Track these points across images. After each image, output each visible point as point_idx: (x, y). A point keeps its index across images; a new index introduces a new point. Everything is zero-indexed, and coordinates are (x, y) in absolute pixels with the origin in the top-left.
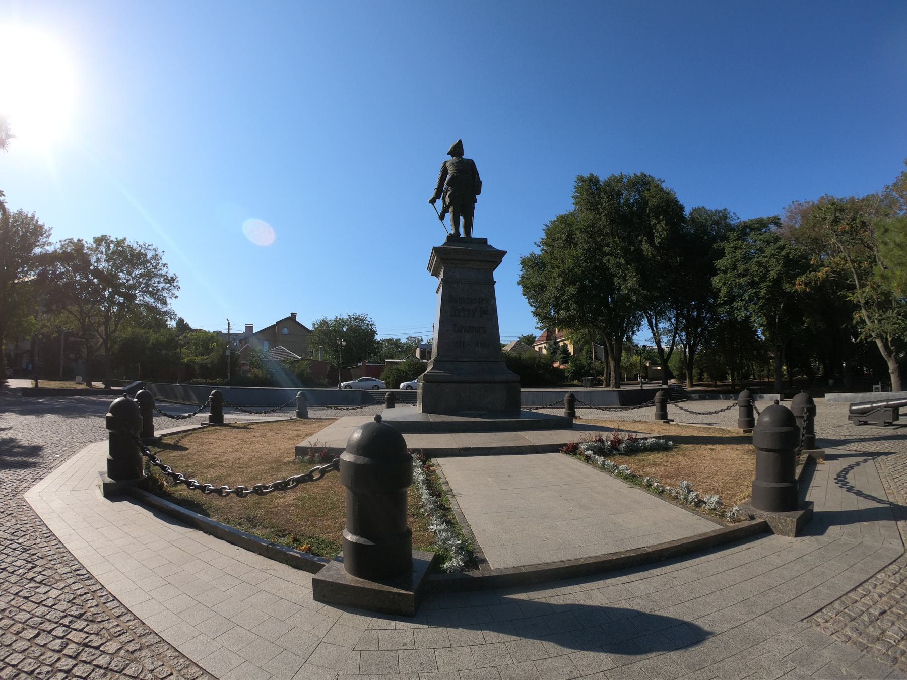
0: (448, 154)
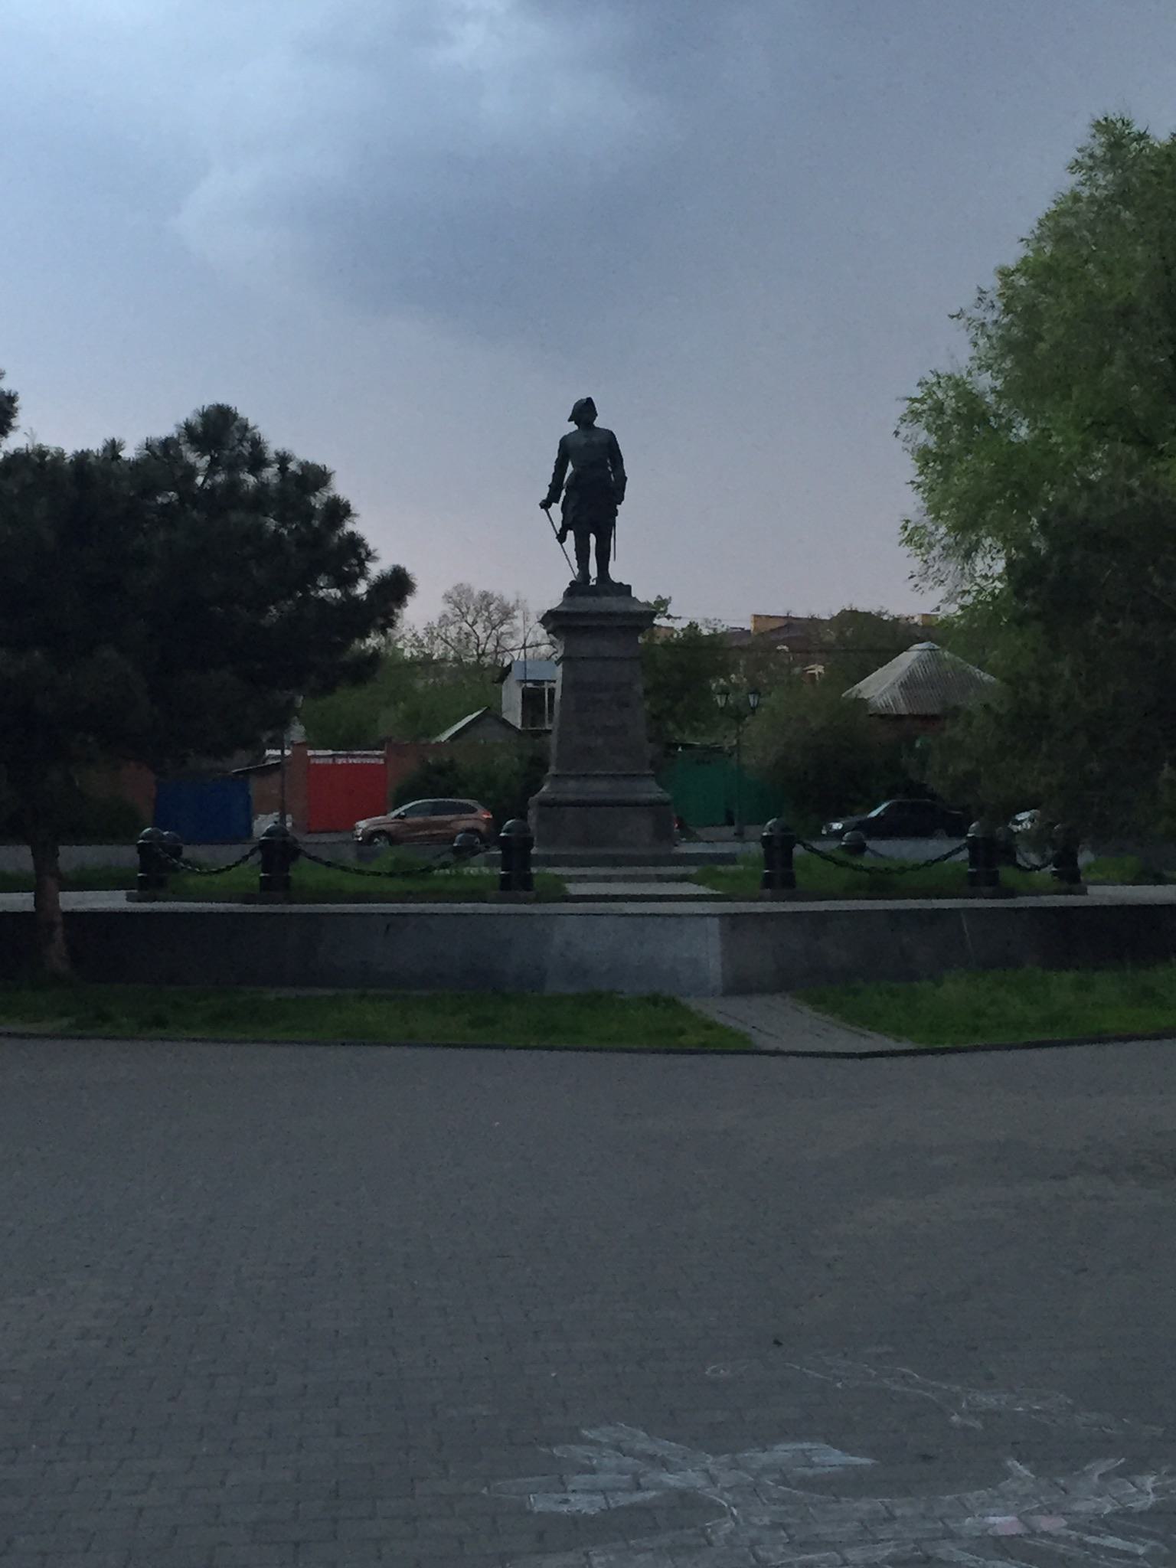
0: (570, 420)
